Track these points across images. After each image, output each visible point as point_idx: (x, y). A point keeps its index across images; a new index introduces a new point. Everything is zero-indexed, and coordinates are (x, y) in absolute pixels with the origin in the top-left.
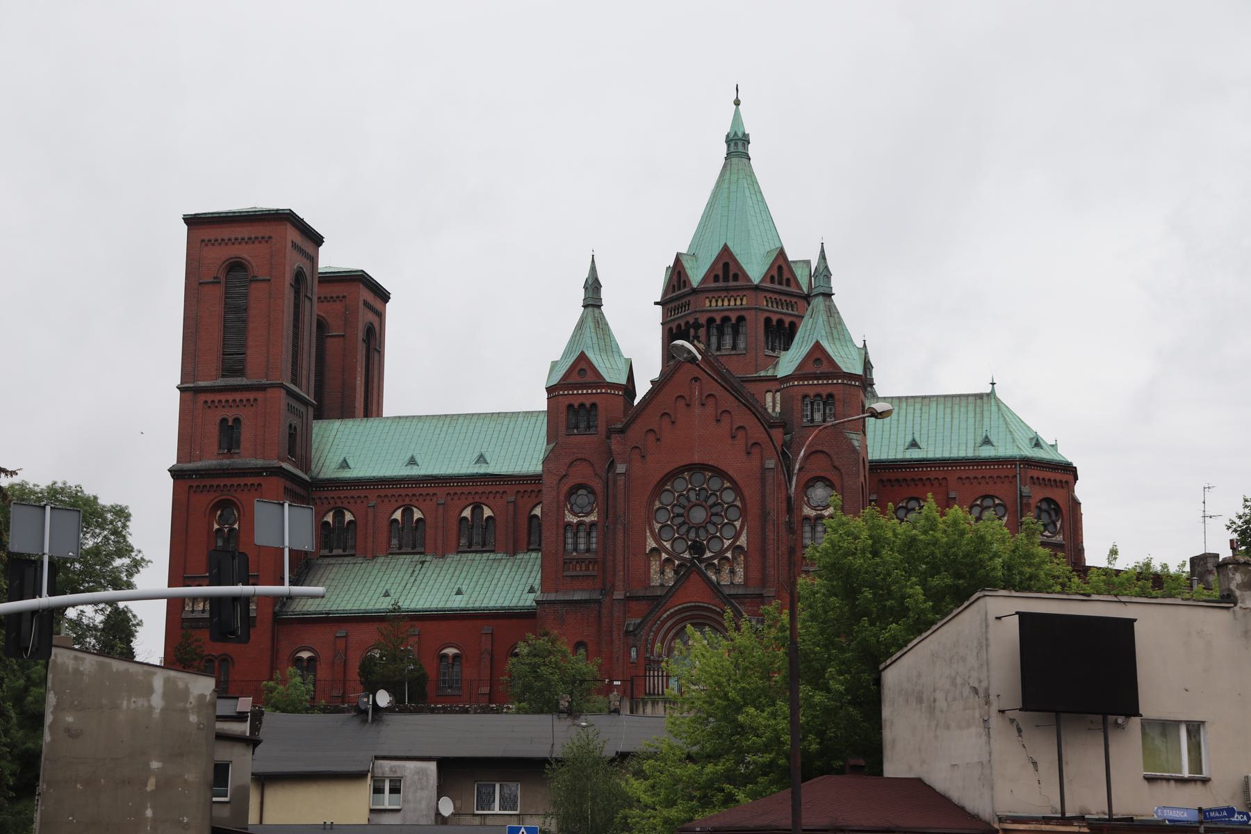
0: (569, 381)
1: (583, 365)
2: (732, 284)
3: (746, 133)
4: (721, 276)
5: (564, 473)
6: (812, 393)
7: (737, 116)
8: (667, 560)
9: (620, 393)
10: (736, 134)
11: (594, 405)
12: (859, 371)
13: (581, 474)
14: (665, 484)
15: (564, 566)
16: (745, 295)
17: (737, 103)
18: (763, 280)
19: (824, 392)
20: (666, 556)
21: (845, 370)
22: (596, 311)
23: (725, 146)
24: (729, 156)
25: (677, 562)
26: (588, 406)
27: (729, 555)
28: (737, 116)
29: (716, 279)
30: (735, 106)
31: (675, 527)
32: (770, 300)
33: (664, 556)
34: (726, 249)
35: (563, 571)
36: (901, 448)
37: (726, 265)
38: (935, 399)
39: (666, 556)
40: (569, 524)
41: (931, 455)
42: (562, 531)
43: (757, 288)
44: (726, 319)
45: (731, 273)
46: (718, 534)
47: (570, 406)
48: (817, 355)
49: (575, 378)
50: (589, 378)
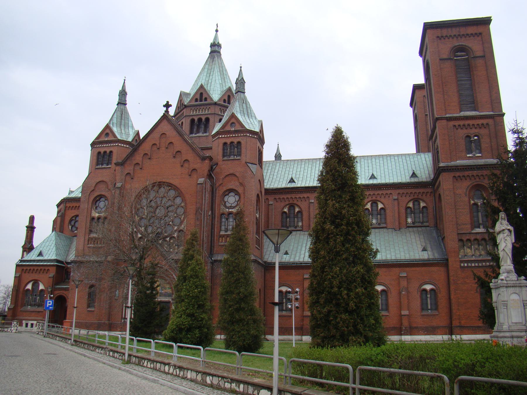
1: (108, 131)
2: (203, 102)
3: (220, 43)
4: (199, 99)
5: (93, 189)
6: (228, 141)
8: (141, 238)
9: (127, 146)
10: (214, 42)
11: (111, 152)
12: (257, 130)
13: (102, 190)
16: (210, 108)
17: (217, 31)
18: (220, 100)
19: (236, 141)
20: (141, 236)
21: (248, 128)
22: (122, 107)
23: (210, 48)
24: (212, 52)
28: (216, 37)
29: (196, 100)
30: (215, 32)
32: (223, 111)
33: (140, 236)
34: (202, 87)
36: (285, 182)
37: (201, 94)
38: (304, 161)
40: (93, 219)
41: (299, 185)
43: (215, 104)
44: (200, 120)
45: (204, 98)
48: (233, 120)
50: (111, 138)
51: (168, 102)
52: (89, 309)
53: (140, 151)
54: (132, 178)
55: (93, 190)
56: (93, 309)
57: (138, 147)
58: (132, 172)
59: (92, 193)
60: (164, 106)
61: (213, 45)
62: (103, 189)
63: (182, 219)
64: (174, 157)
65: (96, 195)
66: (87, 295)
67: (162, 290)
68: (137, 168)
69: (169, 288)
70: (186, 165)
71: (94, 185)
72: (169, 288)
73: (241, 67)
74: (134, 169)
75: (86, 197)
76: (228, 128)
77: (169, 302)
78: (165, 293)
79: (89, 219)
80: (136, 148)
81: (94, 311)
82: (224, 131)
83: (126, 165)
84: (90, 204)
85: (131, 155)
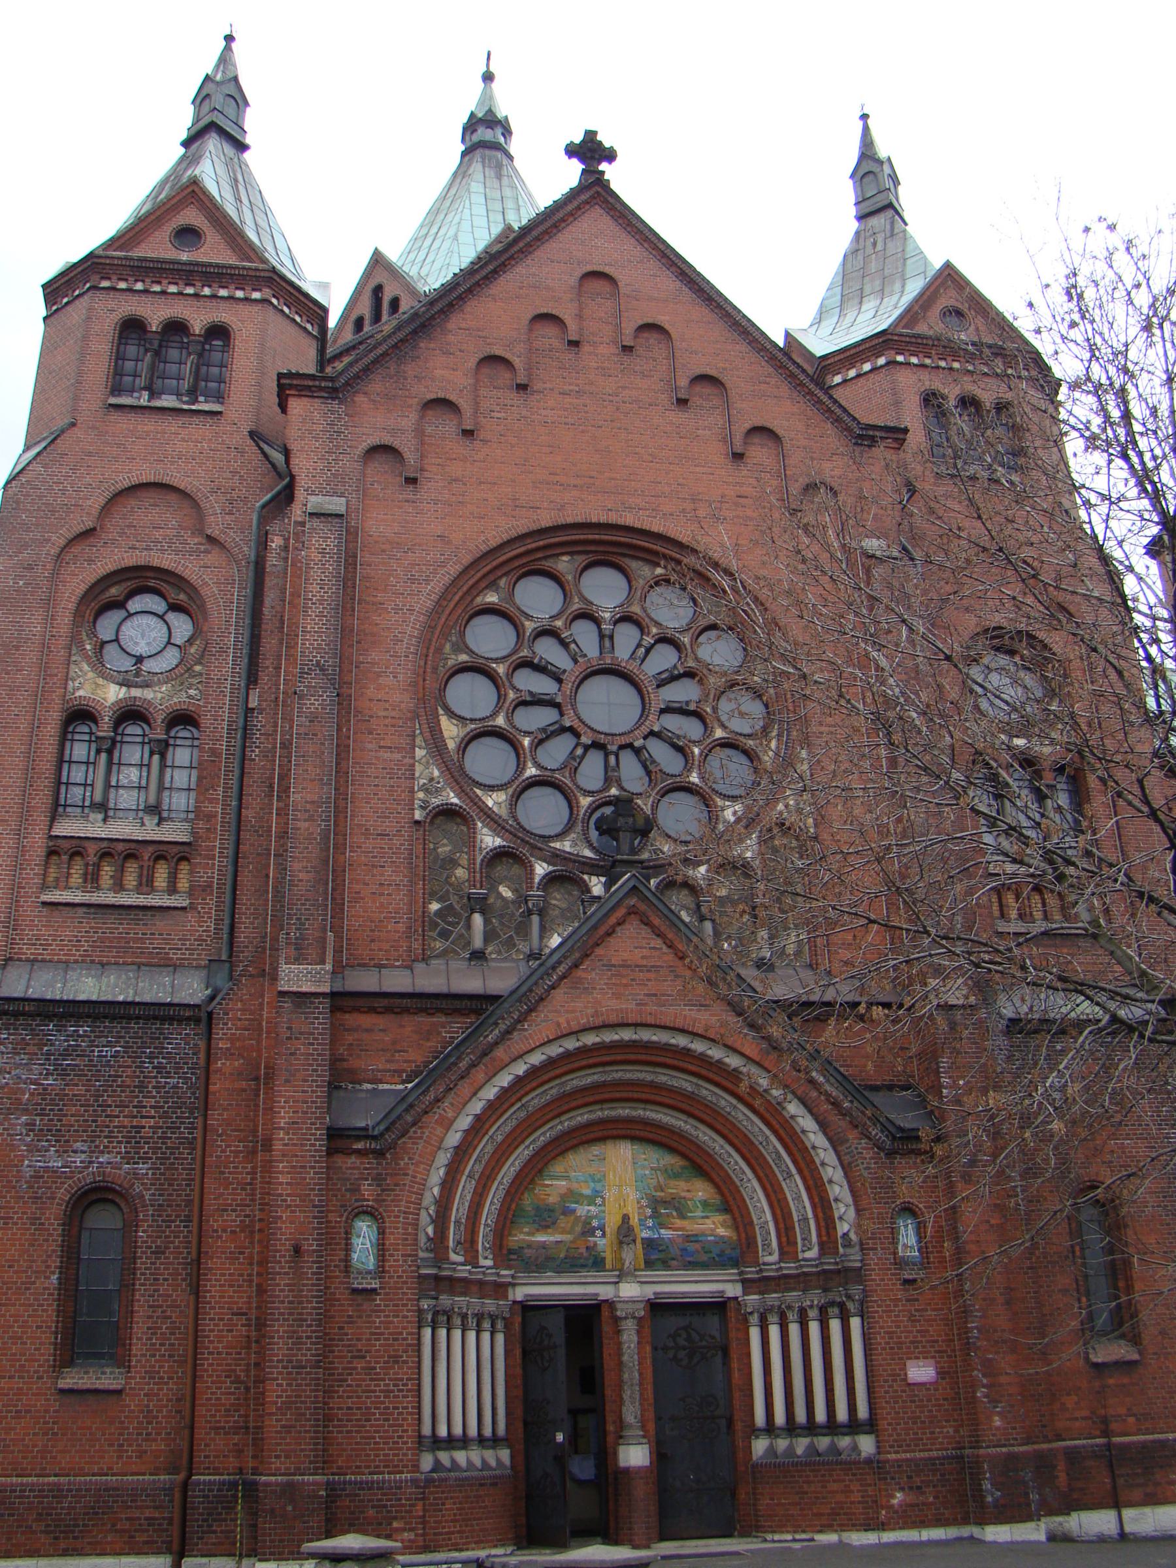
0: (138, 253)
7: (487, 97)
8: (499, 855)
14: (476, 589)
15: (47, 864)
17: (488, 77)
25: (541, 869)
26: (197, 327)
27: (749, 850)
28: (487, 97)
31: (526, 742)
33: (490, 840)
35: (44, 887)
39: (498, 842)
42: (51, 730)
46: (694, 778)
47: (132, 327)
49: (159, 247)
51: (590, 135)
52: (72, 1379)
53: (451, 338)
54: (412, 481)
55: (89, 533)
56: (108, 1378)
57: (442, 311)
58: (406, 445)
59: (76, 550)
60: (572, 151)
61: (472, 125)
62: (157, 534)
63: (768, 758)
64: (682, 402)
65: (111, 567)
66: (55, 1262)
67: (662, 1226)
68: (443, 427)
69: (705, 1204)
70: (760, 453)
71: (96, 502)
72: (705, 1204)
73: (865, 117)
74: (420, 432)
75: (30, 568)
76: (932, 325)
77: (720, 1306)
78: (688, 1238)
79: (55, 717)
80: (432, 318)
81: (119, 1392)
82: (914, 336)
83: (360, 399)
84: (65, 619)
85: (395, 346)
